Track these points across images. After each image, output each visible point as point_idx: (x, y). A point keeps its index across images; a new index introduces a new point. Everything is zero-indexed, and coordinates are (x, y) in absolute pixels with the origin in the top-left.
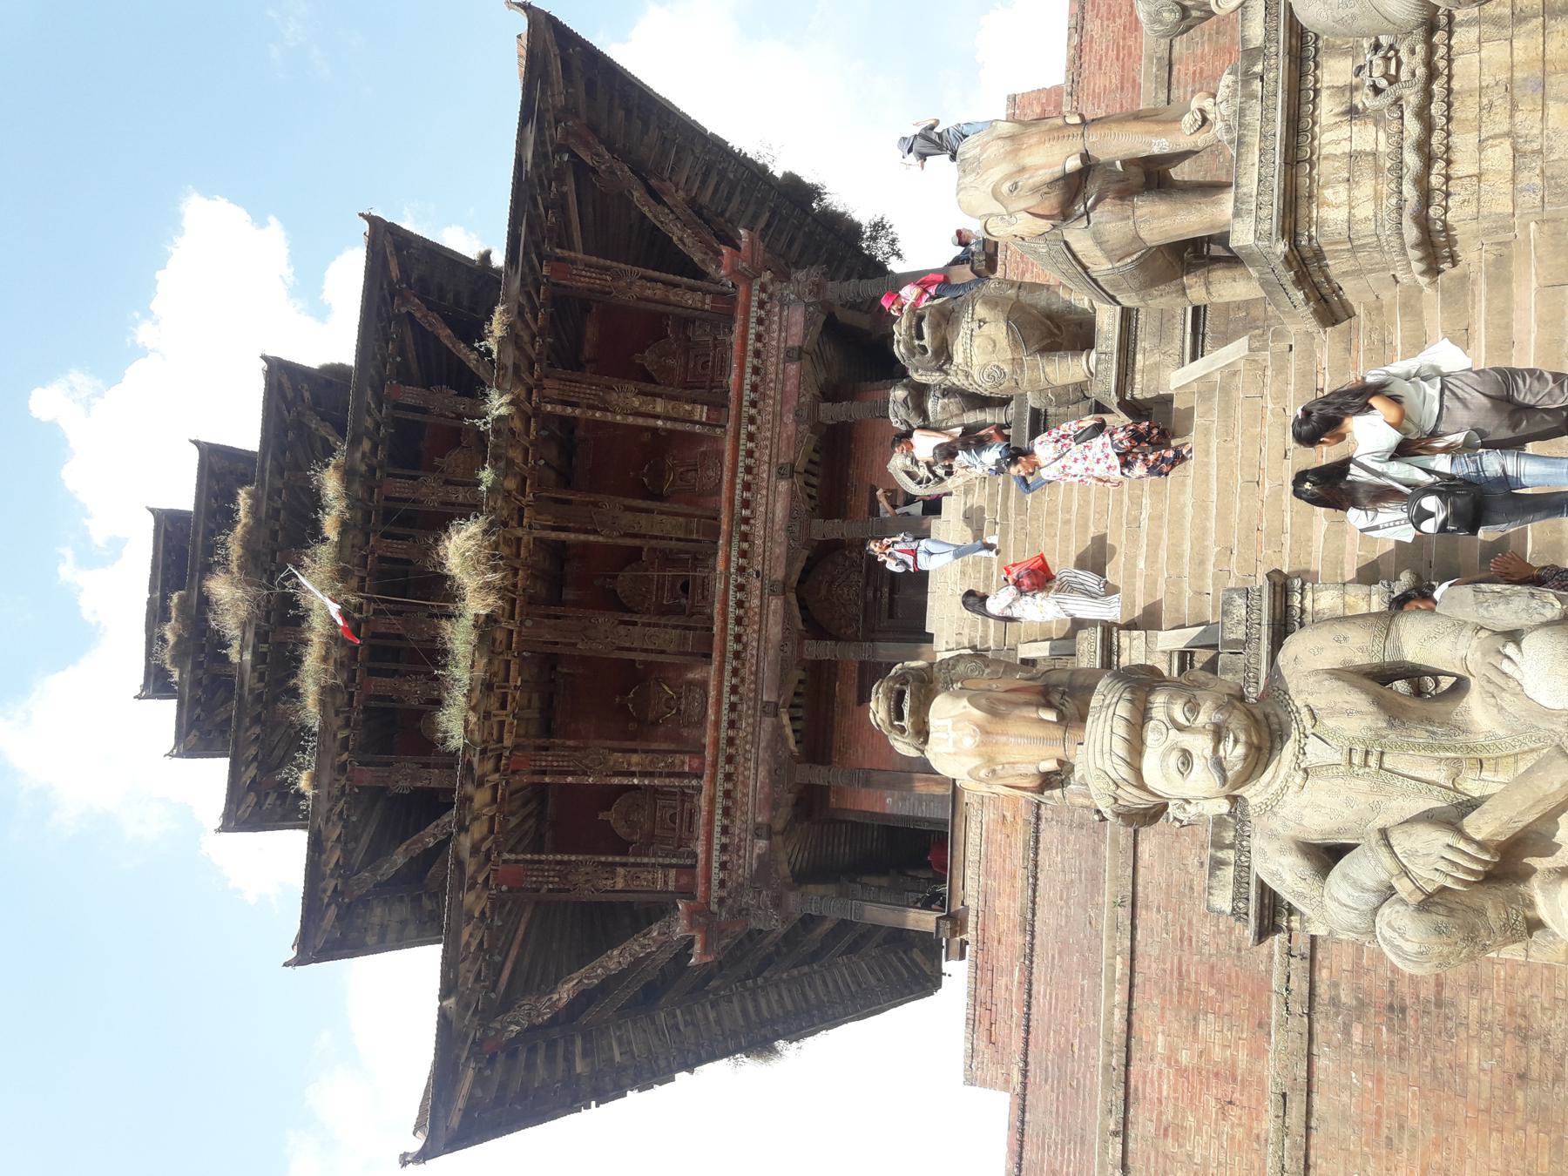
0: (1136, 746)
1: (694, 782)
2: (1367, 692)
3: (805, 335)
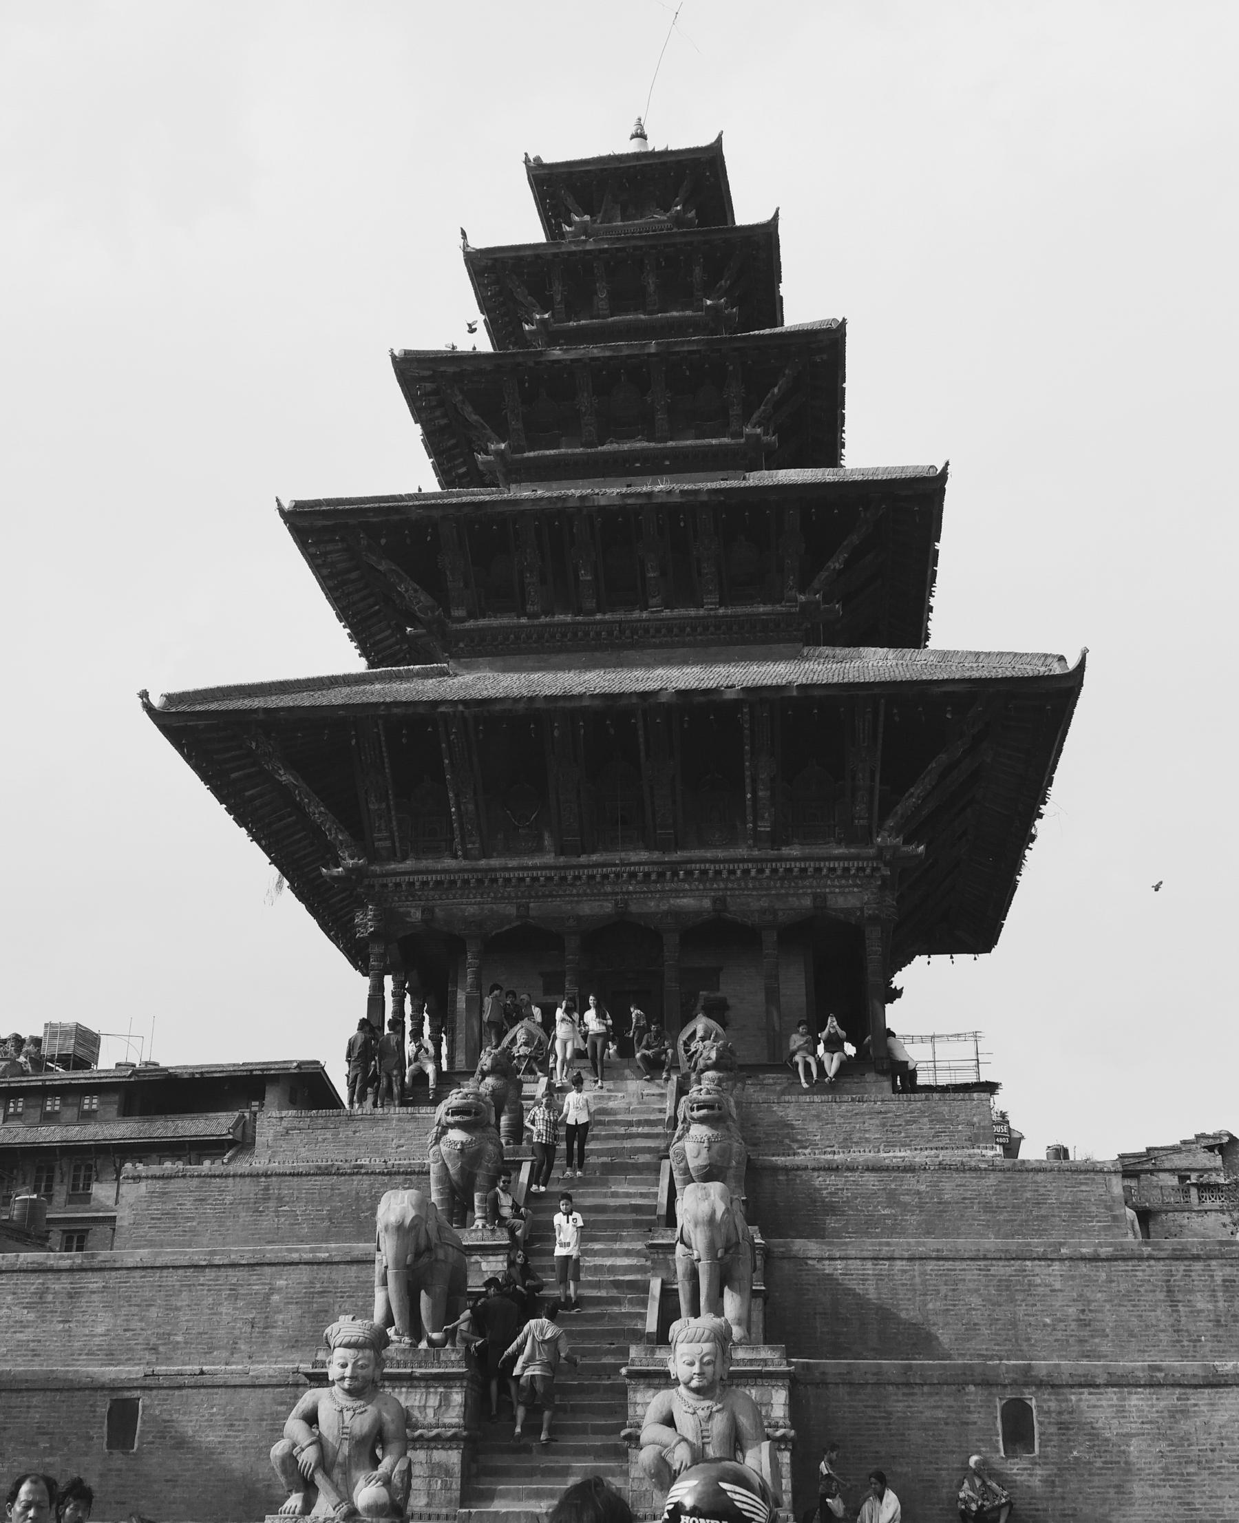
0: (348, 1346)
1: (460, 853)
2: (371, 1431)
3: (835, 910)
